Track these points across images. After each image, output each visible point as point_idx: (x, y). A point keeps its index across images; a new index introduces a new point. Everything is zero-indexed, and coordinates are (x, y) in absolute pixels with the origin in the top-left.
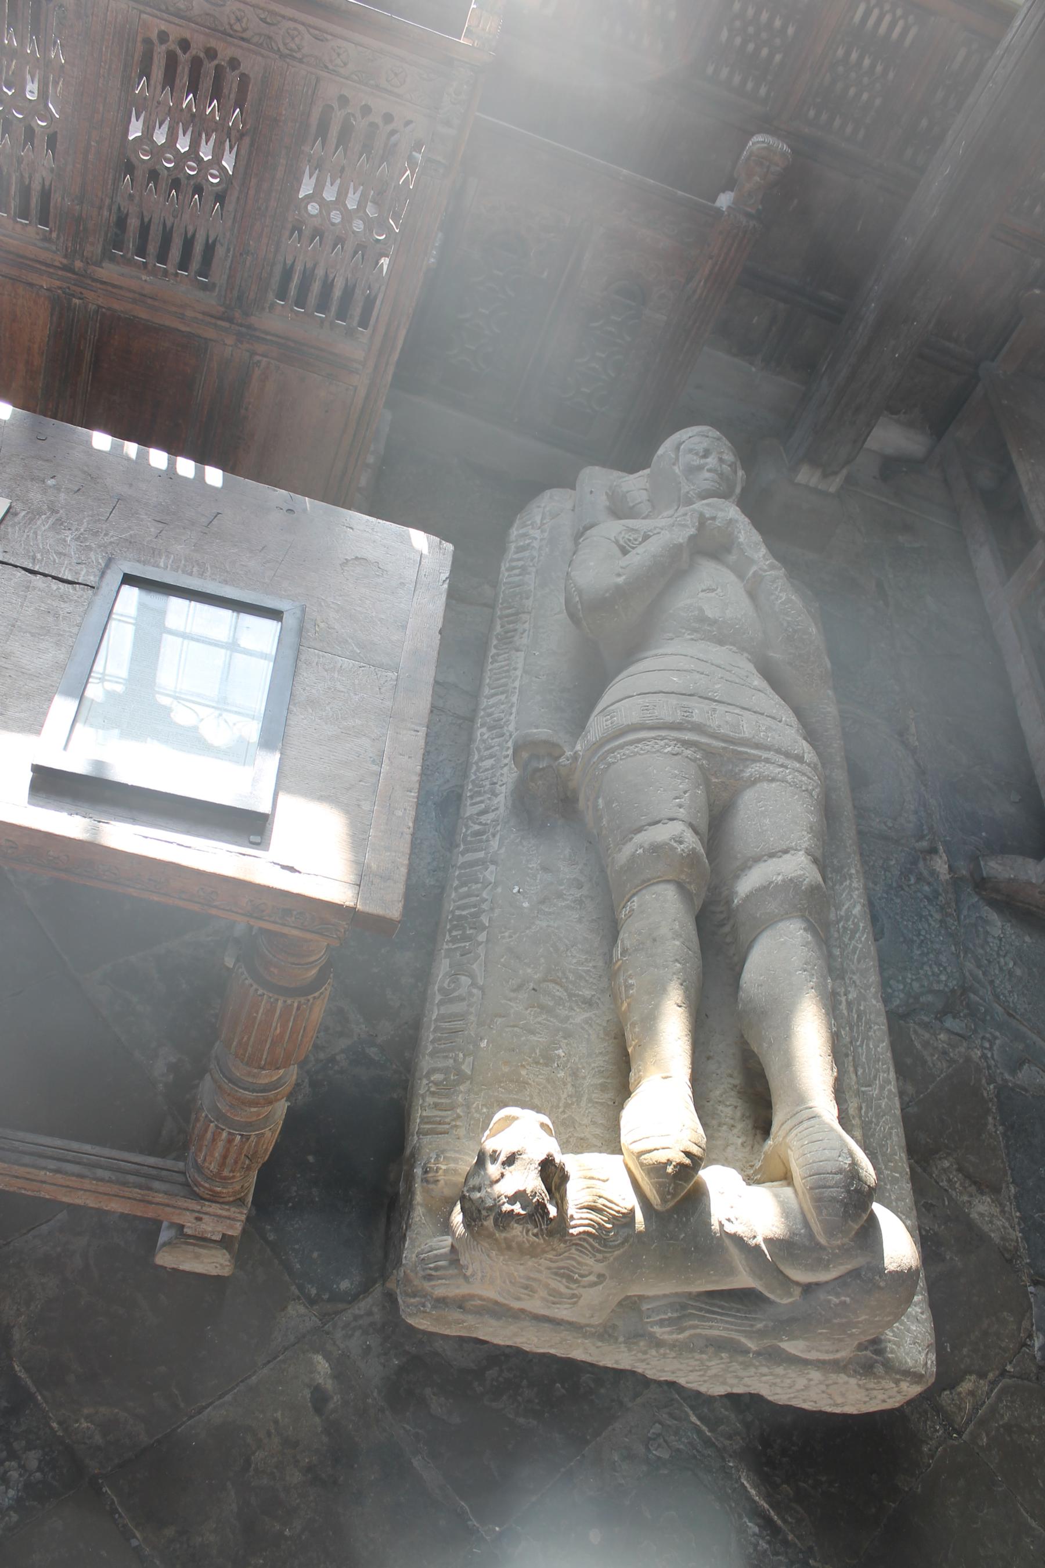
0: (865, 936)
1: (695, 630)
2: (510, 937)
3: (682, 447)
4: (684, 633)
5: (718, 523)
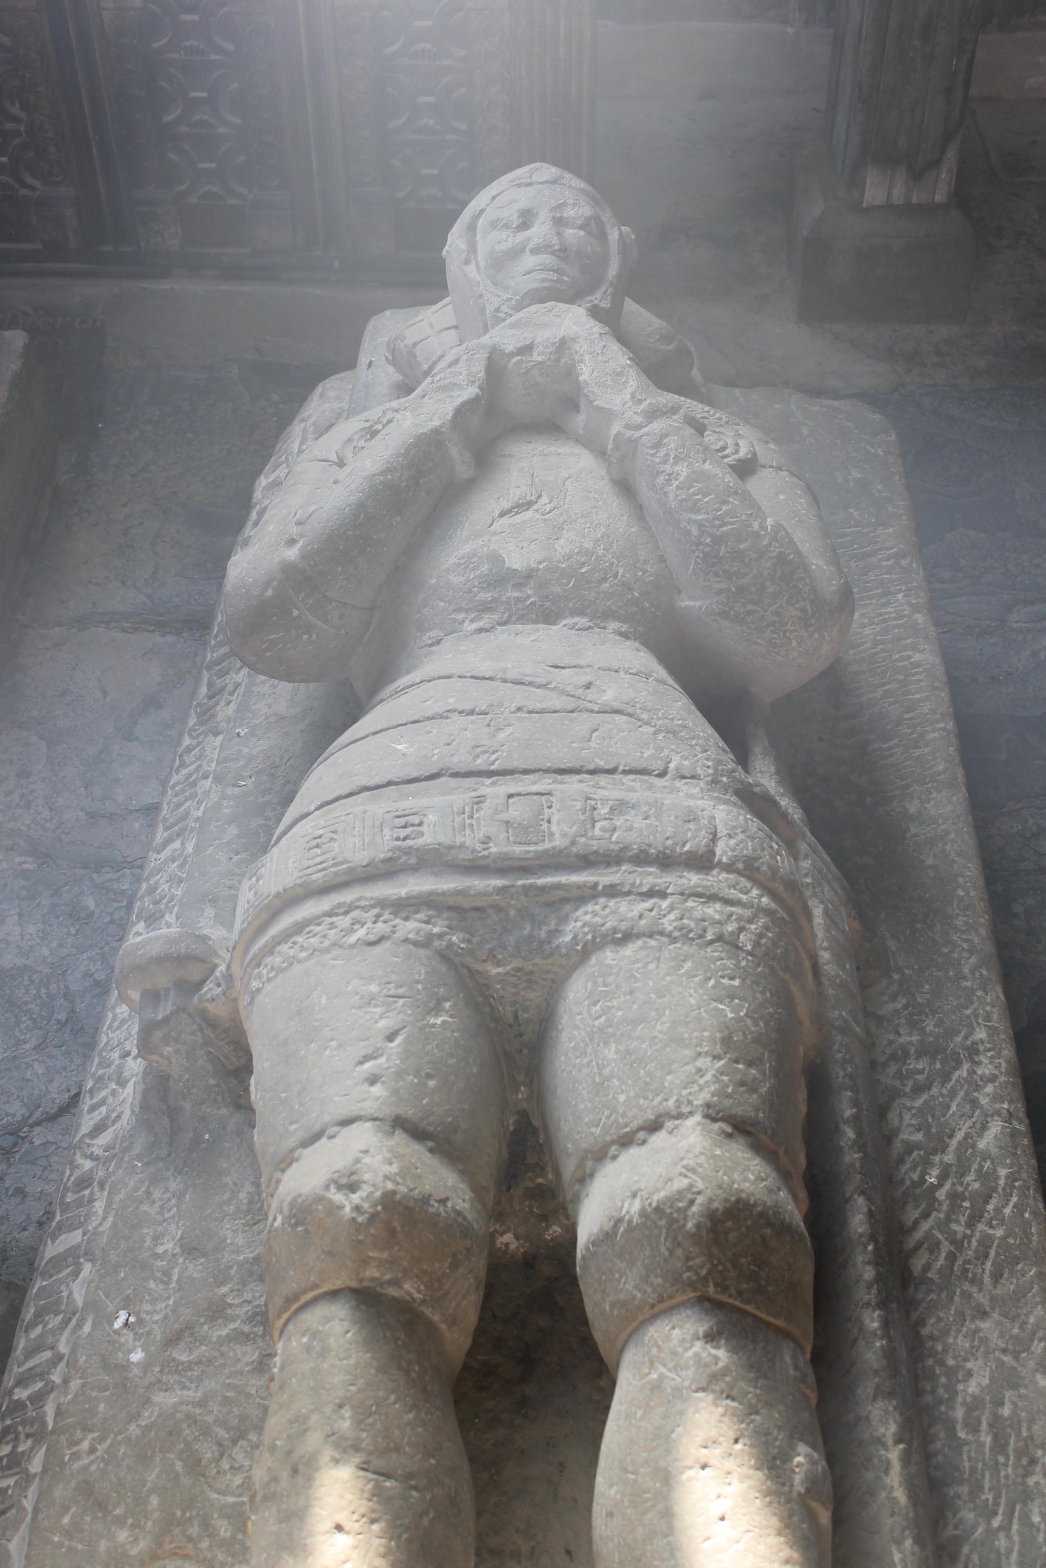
0: (1014, 1199)
1: (486, 608)
2: (92, 1450)
3: (480, 223)
5: (536, 357)
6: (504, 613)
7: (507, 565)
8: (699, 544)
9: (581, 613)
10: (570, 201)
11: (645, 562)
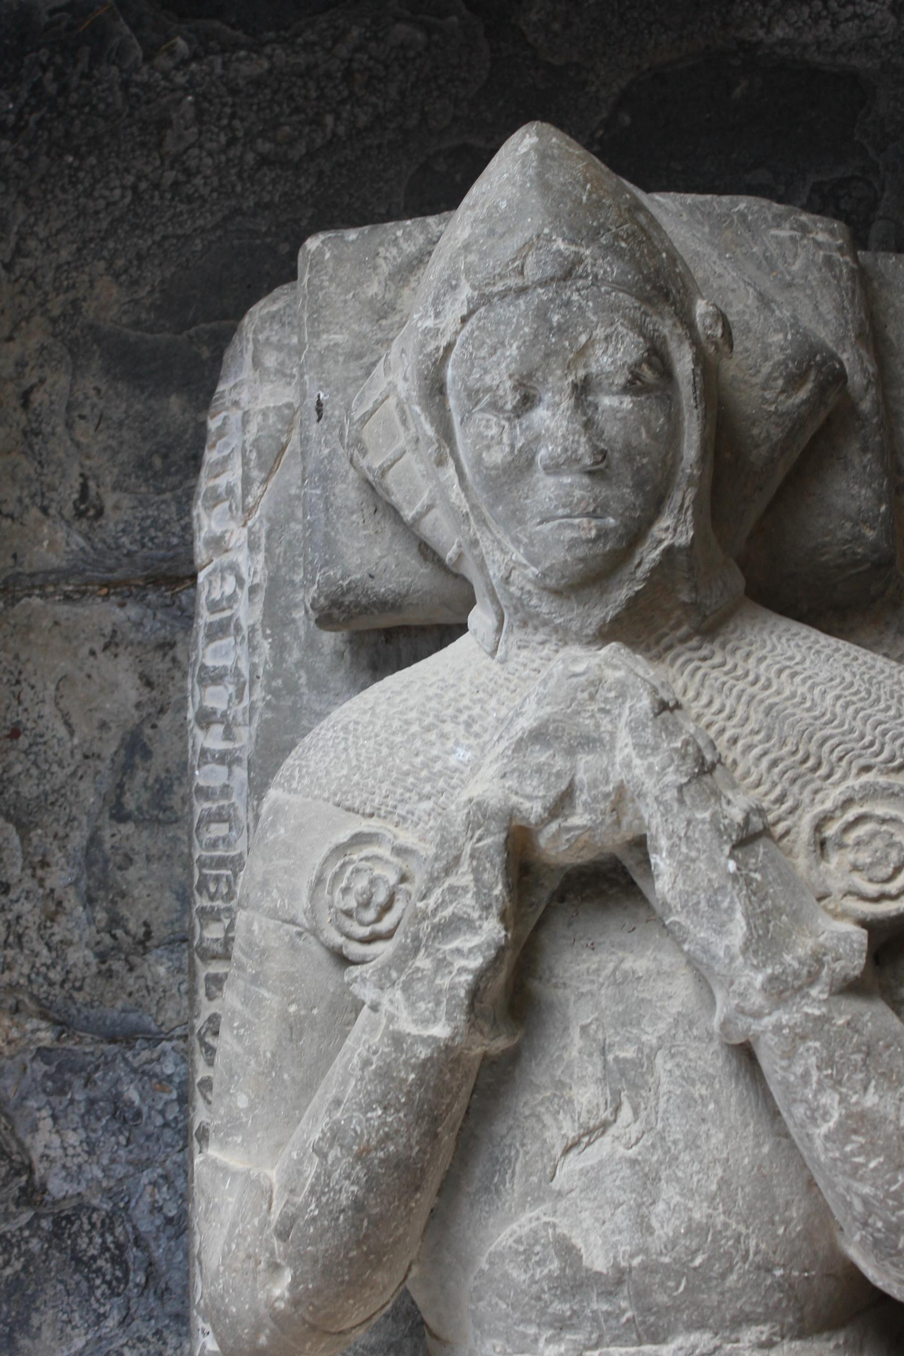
1: (562, 1325)
3: (450, 373)
4: (536, 1340)
6: (591, 1333)
7: (586, 1262)
8: (865, 1224)
9: (699, 1325)
10: (599, 333)
11: (788, 1205)
